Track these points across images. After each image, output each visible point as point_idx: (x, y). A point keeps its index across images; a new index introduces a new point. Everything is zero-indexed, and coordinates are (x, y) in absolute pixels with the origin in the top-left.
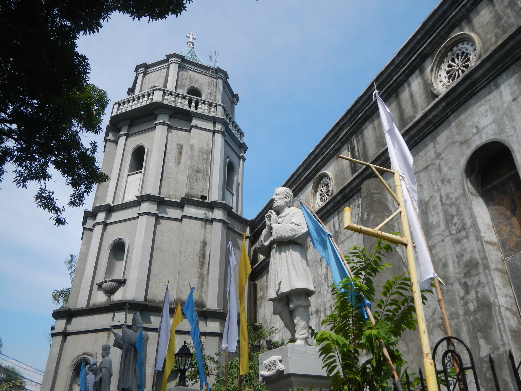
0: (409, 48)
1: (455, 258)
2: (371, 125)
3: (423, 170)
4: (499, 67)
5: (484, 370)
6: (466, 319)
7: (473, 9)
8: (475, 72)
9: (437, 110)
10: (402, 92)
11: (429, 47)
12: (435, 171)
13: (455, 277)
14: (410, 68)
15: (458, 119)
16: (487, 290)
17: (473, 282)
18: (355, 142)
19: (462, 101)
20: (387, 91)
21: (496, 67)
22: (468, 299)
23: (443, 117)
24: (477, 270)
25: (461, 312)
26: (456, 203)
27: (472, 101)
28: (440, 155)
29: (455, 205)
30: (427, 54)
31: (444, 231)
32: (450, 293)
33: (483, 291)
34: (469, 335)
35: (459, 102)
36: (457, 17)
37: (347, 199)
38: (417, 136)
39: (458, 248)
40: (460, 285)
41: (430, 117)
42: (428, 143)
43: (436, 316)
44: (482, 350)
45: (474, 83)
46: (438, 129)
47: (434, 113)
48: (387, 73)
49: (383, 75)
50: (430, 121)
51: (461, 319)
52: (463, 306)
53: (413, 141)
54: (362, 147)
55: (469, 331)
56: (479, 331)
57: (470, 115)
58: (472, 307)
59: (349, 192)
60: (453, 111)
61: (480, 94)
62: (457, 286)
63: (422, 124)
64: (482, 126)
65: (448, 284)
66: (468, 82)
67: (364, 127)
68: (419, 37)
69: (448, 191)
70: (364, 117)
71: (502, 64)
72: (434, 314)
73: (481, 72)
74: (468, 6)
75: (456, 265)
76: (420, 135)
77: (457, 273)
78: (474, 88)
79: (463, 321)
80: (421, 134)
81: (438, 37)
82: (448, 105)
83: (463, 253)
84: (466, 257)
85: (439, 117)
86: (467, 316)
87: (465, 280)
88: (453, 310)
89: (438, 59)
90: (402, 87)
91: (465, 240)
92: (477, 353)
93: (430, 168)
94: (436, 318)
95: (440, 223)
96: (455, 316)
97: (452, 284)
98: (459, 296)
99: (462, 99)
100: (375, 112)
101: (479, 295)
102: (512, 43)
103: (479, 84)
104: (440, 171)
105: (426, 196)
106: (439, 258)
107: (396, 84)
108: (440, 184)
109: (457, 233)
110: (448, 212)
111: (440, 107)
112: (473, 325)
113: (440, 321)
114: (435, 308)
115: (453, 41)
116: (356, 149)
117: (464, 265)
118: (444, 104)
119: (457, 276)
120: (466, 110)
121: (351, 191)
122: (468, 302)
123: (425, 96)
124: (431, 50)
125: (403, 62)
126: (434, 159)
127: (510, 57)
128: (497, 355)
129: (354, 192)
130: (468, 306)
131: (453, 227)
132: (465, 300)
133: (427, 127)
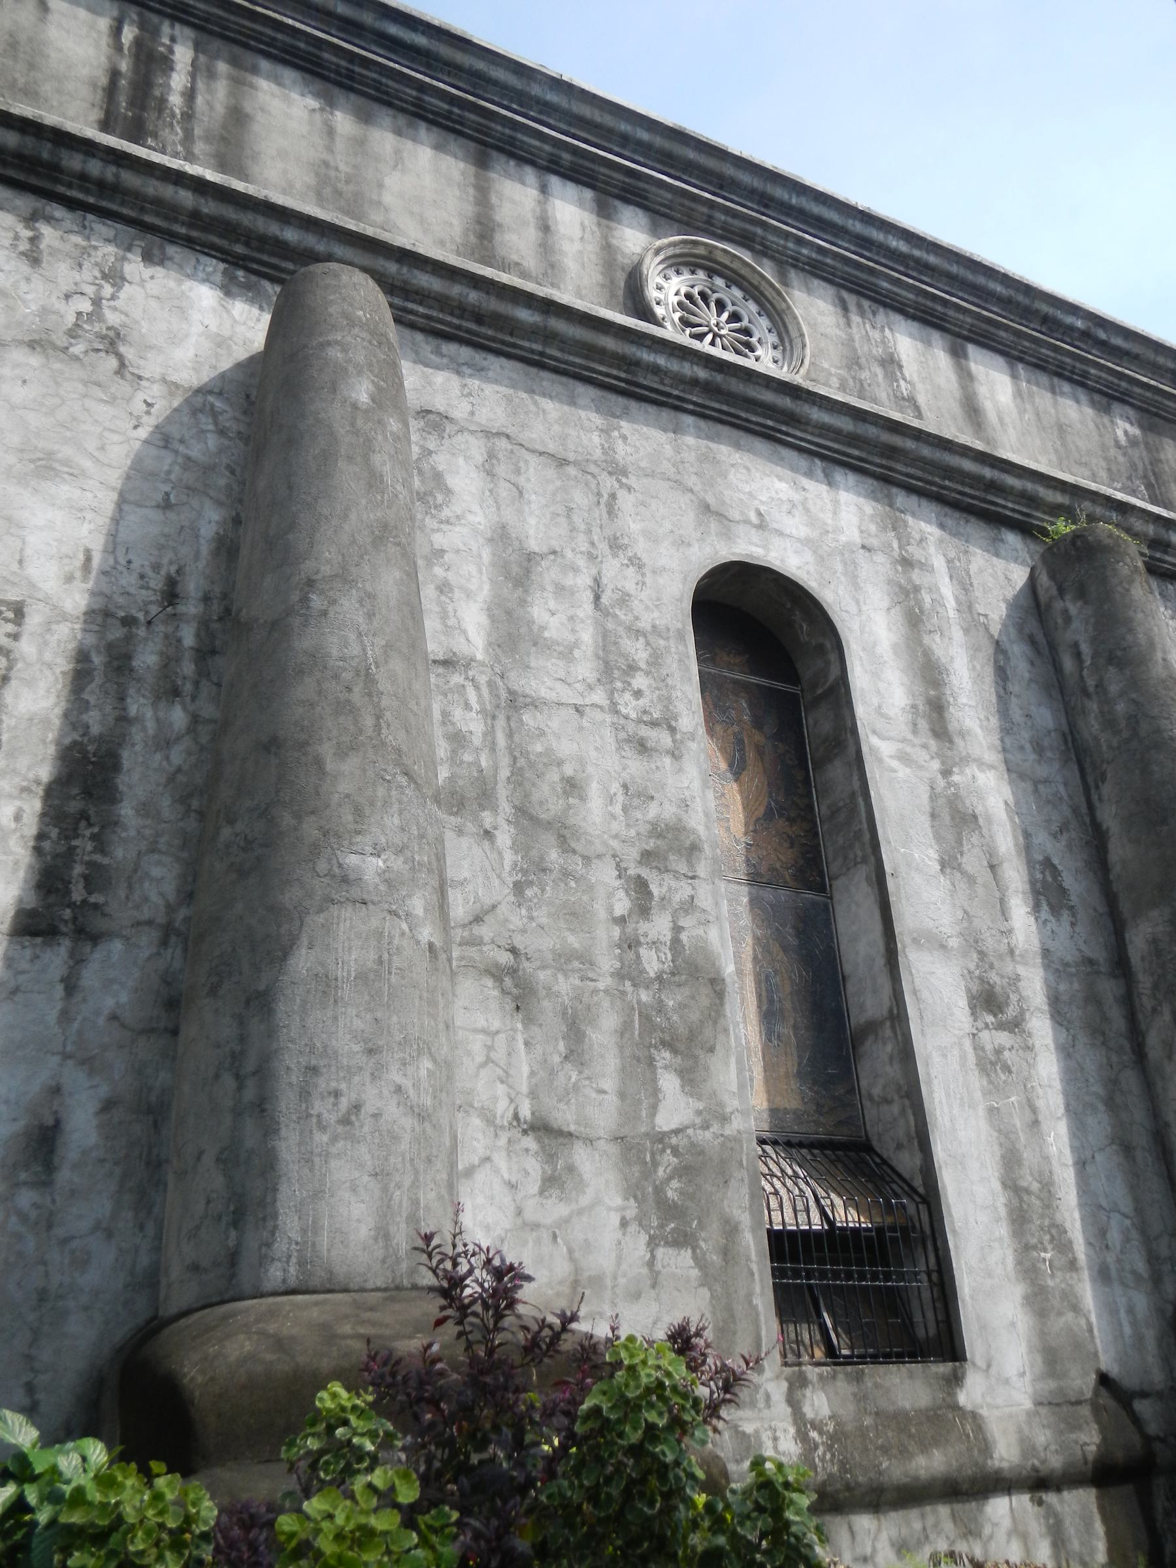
0: (597, 116)
1: (615, 787)
2: (313, 103)
3: (541, 454)
4: (856, 452)
5: (661, 1172)
6: (623, 993)
7: (803, 270)
8: (814, 403)
9: (674, 365)
10: (508, 176)
11: (669, 196)
12: (593, 499)
13: (605, 844)
14: (581, 161)
15: (711, 445)
16: (713, 935)
17: (670, 889)
18: (183, 55)
19: (738, 417)
20: (460, 107)
21: (850, 445)
22: (641, 932)
23: (669, 395)
24: (691, 865)
25: (607, 963)
26: (650, 637)
27: (760, 444)
28: (625, 473)
29: (648, 644)
30: (646, 198)
31: (590, 688)
32: (573, 884)
33: (700, 932)
34: (621, 1048)
35: (732, 411)
36: (771, 237)
37: (33, 181)
38: (562, 350)
39: (636, 766)
40: (620, 877)
41: (647, 356)
42: (581, 401)
43: (485, 931)
44: (661, 1108)
45: (793, 419)
46: (633, 405)
47: (661, 361)
48: (481, 65)
49: (463, 50)
50: (633, 364)
51: (601, 985)
52: (619, 946)
53: (537, 347)
54: (220, 109)
55: (624, 1030)
56: (663, 1043)
57: (748, 469)
58: (652, 962)
59: (83, 177)
60: (701, 414)
61: (786, 452)
62: (605, 875)
63: (609, 343)
64: (775, 526)
65: (574, 852)
66: (786, 402)
67: (265, 64)
68: (644, 135)
69: (630, 586)
70: (302, 45)
71: (863, 455)
72: (478, 919)
73: (826, 418)
74: (805, 251)
75: (617, 809)
76: (571, 358)
77: (616, 836)
78: (784, 428)
79: (606, 991)
80: (578, 360)
81: (705, 210)
82: (708, 388)
83: (652, 792)
84: (662, 810)
85: (662, 383)
86: (628, 983)
87: (645, 873)
88: (573, 941)
89: (678, 251)
90: (512, 163)
91: (667, 761)
92: (644, 1113)
93: (572, 471)
94: (486, 939)
95: (577, 653)
96: (576, 964)
97: (587, 859)
98: (610, 909)
99: (743, 415)
100: (351, 89)
101: (684, 937)
102: (910, 444)
103: (798, 434)
104: (611, 511)
105: (532, 532)
106: (548, 752)
107: (507, 131)
108: (603, 547)
109: (640, 721)
110: (616, 643)
111: (688, 369)
112: (646, 1018)
113: (505, 958)
114: (488, 901)
115: (735, 265)
116: (178, 80)
117: (649, 827)
118: (702, 374)
119: (615, 844)
120: (737, 446)
121: (102, 187)
122: (639, 943)
123: (600, 278)
124: (665, 206)
125: (549, 116)
126: (595, 462)
127: (884, 462)
128: (716, 1136)
129: (114, 207)
130: (638, 957)
131: (627, 696)
132: (630, 928)
133: (611, 366)
